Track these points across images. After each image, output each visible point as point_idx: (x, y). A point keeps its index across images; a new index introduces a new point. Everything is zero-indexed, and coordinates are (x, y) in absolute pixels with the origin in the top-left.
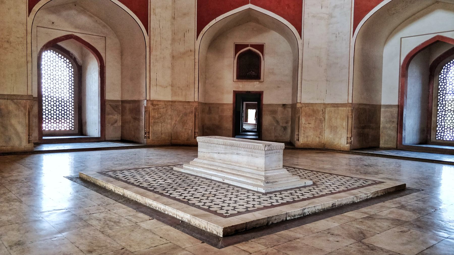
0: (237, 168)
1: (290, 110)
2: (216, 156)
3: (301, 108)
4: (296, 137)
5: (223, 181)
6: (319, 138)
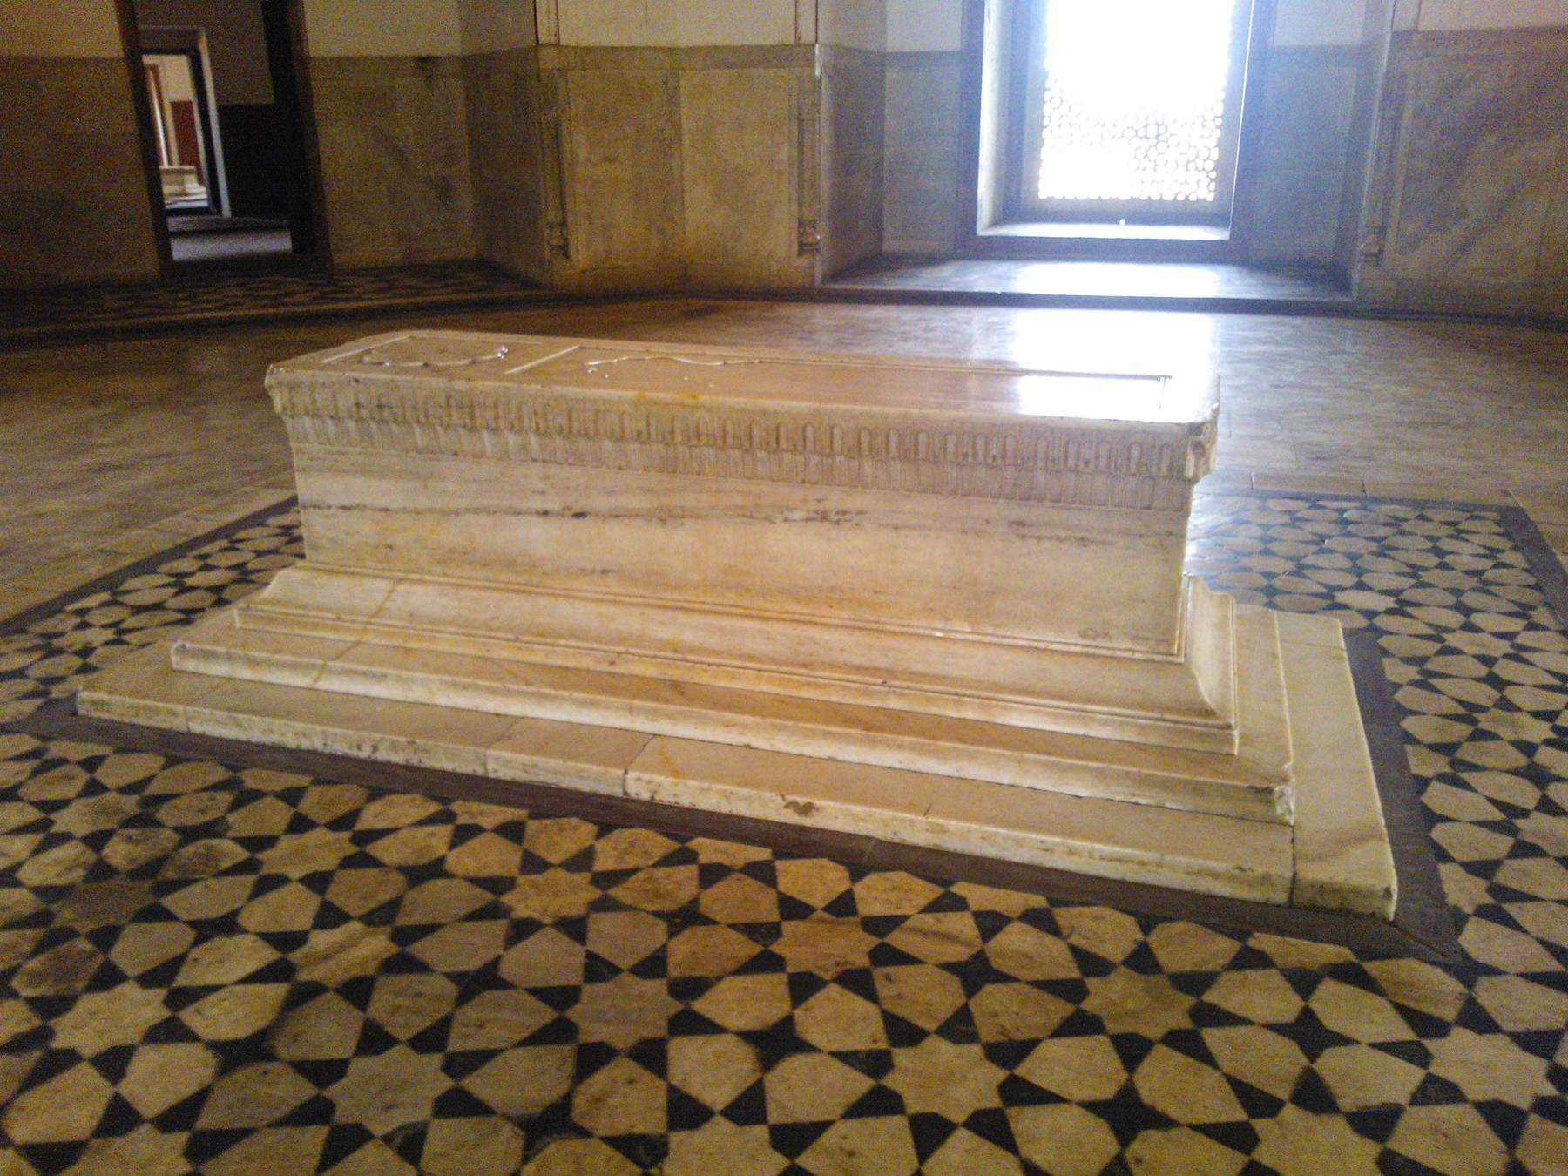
0: (835, 642)
1: (456, 88)
2: (537, 537)
3: (563, 71)
4: (552, 238)
5: (791, 818)
6: (660, 231)
